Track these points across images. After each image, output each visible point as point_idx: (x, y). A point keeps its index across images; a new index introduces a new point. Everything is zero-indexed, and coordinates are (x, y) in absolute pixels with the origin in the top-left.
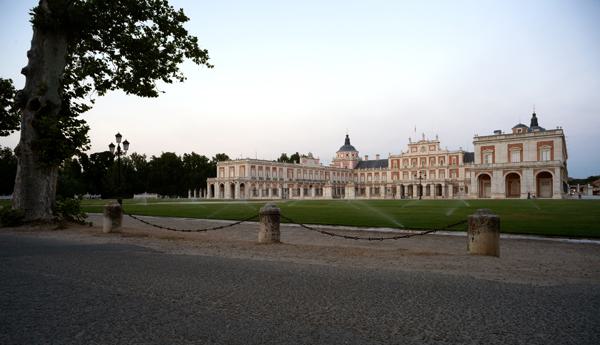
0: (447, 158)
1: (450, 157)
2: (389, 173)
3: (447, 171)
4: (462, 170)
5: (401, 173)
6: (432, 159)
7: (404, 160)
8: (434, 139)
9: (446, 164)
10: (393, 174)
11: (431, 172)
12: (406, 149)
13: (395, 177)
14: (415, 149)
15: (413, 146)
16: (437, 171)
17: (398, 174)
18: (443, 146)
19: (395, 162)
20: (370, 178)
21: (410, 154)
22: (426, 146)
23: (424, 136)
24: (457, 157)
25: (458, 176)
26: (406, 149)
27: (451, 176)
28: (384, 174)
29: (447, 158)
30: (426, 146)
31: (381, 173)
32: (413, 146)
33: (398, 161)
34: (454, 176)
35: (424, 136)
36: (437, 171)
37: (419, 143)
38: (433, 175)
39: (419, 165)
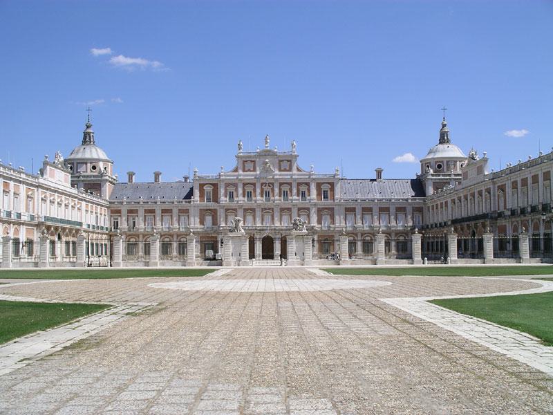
1: (319, 186)
15: (247, 162)
27: (319, 222)
33: (215, 186)
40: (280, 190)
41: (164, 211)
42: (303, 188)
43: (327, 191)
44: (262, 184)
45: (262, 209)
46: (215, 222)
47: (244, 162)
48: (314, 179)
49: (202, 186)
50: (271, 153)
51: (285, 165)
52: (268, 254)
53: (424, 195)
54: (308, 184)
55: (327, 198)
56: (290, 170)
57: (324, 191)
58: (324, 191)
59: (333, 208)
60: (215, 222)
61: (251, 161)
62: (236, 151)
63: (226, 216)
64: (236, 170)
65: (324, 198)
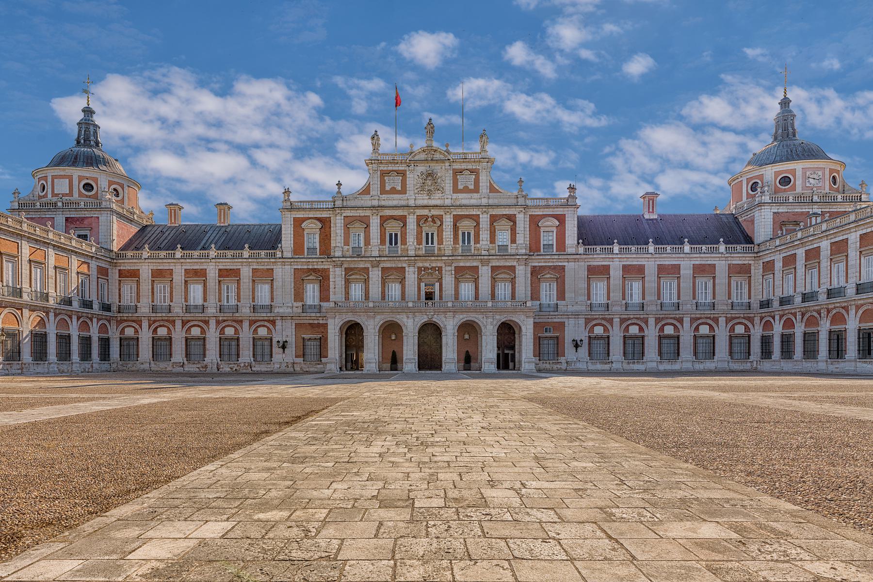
2: (284, 274)
3: (522, 273)
4: (576, 271)
5: (337, 277)
7: (349, 222)
9: (523, 238)
10: (300, 278)
11: (460, 273)
13: (312, 292)
14: (395, 182)
17: (323, 278)
20: (196, 292)
22: (444, 173)
24: (561, 219)
25: (561, 295)
28: (265, 275)
30: (444, 173)
33: (325, 224)
34: (548, 292)
38: (467, 289)
40: (456, 228)
41: (224, 274)
44: (419, 218)
45: (419, 269)
46: (324, 295)
47: (384, 174)
48: (526, 207)
49: (298, 223)
50: (437, 156)
52: (429, 362)
53: (749, 240)
54: (511, 218)
59: (563, 268)
60: (324, 295)
61: (398, 172)
64: (366, 191)
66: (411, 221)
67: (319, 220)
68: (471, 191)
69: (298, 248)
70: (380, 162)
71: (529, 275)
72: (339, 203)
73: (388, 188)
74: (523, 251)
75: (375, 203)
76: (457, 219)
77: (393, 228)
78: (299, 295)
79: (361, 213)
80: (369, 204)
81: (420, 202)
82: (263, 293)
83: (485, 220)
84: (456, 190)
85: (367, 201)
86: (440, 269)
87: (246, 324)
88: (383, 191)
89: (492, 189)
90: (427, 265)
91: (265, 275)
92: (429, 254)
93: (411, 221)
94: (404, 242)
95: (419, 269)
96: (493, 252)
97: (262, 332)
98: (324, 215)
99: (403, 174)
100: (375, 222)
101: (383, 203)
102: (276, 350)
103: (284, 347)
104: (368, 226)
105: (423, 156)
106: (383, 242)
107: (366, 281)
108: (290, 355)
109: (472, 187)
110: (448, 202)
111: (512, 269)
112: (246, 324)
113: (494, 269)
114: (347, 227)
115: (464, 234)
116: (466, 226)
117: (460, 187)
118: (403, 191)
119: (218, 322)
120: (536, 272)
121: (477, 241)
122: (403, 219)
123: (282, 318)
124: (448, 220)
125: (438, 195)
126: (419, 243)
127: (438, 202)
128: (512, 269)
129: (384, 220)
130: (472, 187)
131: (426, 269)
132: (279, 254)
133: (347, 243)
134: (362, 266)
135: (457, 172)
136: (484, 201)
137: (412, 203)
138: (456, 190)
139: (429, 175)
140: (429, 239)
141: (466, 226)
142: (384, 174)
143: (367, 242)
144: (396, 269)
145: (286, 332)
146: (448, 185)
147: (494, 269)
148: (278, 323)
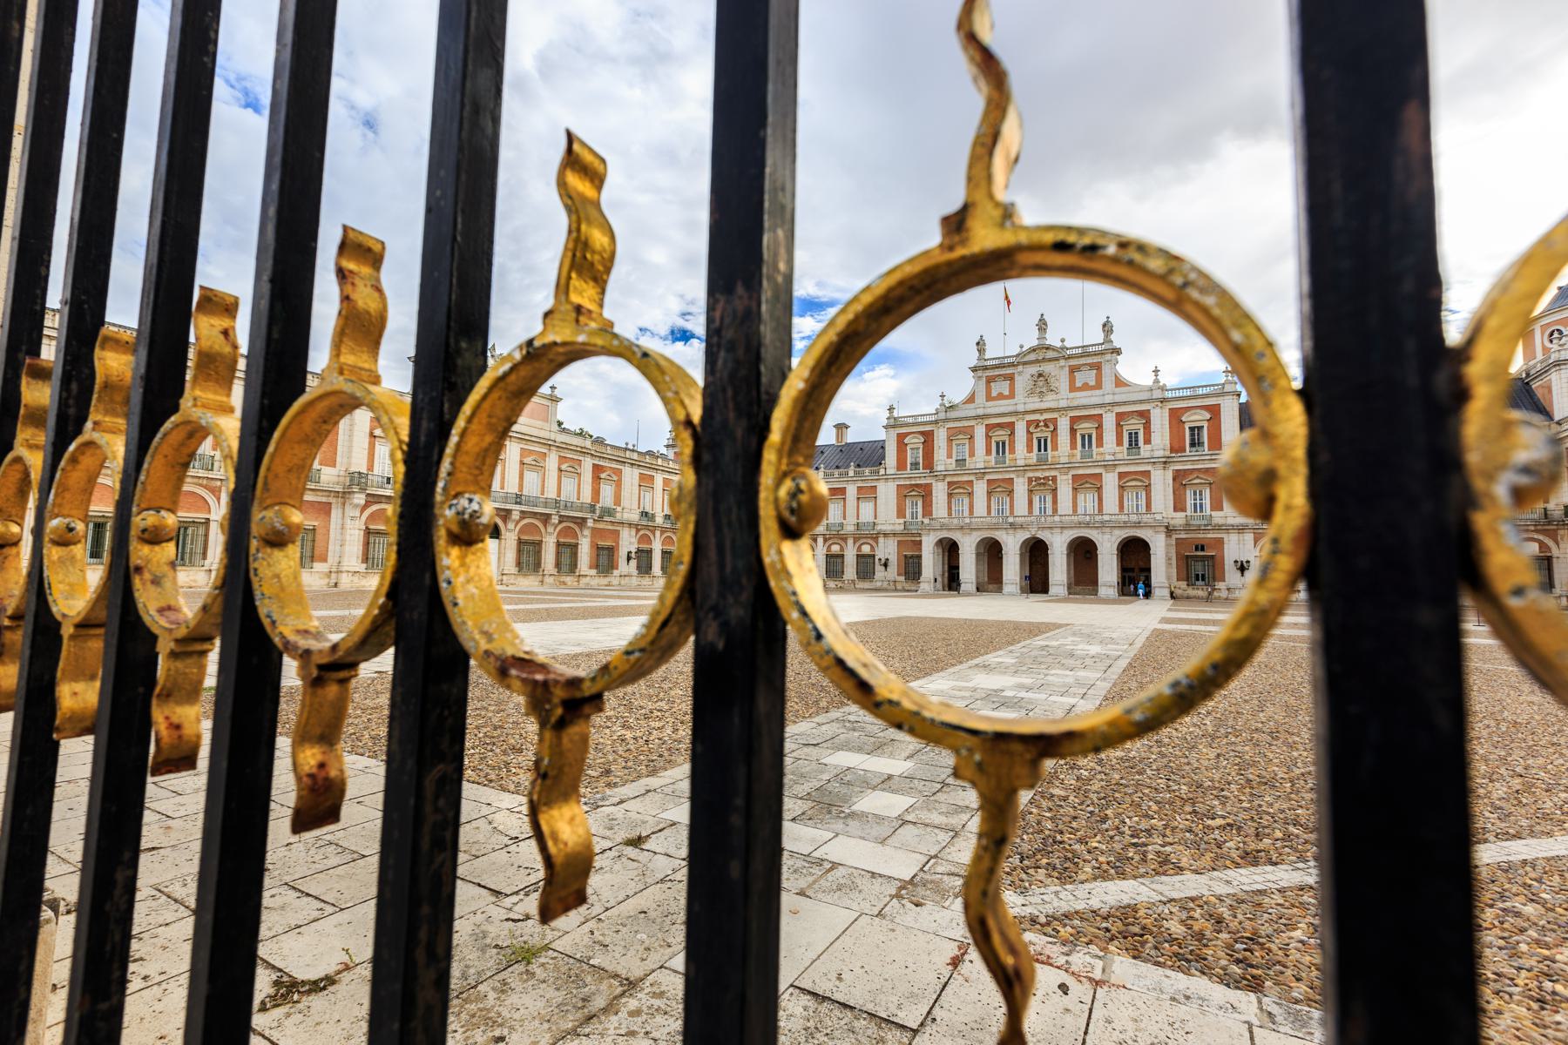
0: (1160, 420)
1: (1176, 417)
2: (887, 492)
3: (1162, 482)
5: (940, 491)
6: (1086, 428)
8: (1095, 337)
10: (903, 493)
11: (1080, 483)
12: (961, 386)
13: (915, 507)
14: (1002, 387)
15: (992, 372)
16: (1110, 482)
17: (926, 493)
18: (1135, 369)
19: (915, 442)
21: (982, 406)
23: (1042, 325)
24: (1215, 411)
26: (961, 386)
27: (1179, 506)
28: (868, 493)
29: (1160, 420)
30: (1058, 374)
31: (852, 491)
32: (992, 372)
33: (928, 437)
35: (1042, 325)
36: (1110, 482)
37: (1021, 360)
38: (1087, 501)
39: (1022, 453)
40: (1073, 431)
42: (1135, 424)
43: (1200, 428)
44: (1029, 423)
46: (928, 511)
48: (1164, 401)
49: (901, 438)
50: (1050, 354)
51: (1089, 377)
54: (1145, 415)
55: (1200, 444)
56: (1098, 386)
57: (1192, 429)
58: (1192, 429)
62: (973, 361)
63: (950, 495)
64: (971, 399)
65: (1193, 445)
66: (1020, 429)
67: (922, 433)
68: (1092, 388)
69: (901, 465)
70: (986, 368)
71: (1171, 481)
72: (942, 416)
73: (994, 394)
74: (1161, 453)
75: (980, 412)
76: (1074, 420)
77: (1001, 435)
78: (901, 513)
79: (966, 423)
80: (972, 413)
81: (1030, 407)
82: (867, 510)
83: (1109, 421)
84: (1073, 388)
85: (970, 411)
86: (1054, 479)
87: (850, 541)
88: (989, 398)
89: (1119, 382)
90: (1039, 474)
91: (868, 493)
92: (1042, 461)
93: (1020, 429)
94: (1012, 451)
95: (1030, 480)
96: (1119, 456)
97: (866, 549)
98: (928, 428)
99: (1011, 378)
100: (980, 432)
101: (989, 411)
102: (879, 568)
103: (886, 565)
104: (972, 437)
105: (1032, 357)
106: (988, 452)
107: (970, 494)
108: (893, 571)
109: (1092, 383)
110: (1063, 404)
111: (1147, 474)
112: (850, 541)
113: (1121, 476)
114: (950, 440)
115: (1083, 437)
116: (1086, 427)
117: (1078, 384)
118: (1012, 396)
119: (825, 540)
120: (1178, 476)
121: (1100, 444)
122: (1011, 426)
123: (886, 535)
124: (1064, 424)
125: (1051, 396)
126: (1030, 450)
127: (1052, 405)
128: (1147, 474)
129: (989, 428)
130: (1092, 383)
131: (1038, 479)
132: (882, 472)
133: (949, 456)
134: (965, 478)
135: (1073, 370)
136: (1108, 399)
137: (1021, 408)
138: (1073, 388)
139: (1040, 375)
140: (1042, 445)
141: (1086, 427)
142: (989, 380)
143: (972, 454)
144: (1003, 480)
145: (887, 549)
146: (1063, 383)
147: (1121, 476)
148: (881, 540)
